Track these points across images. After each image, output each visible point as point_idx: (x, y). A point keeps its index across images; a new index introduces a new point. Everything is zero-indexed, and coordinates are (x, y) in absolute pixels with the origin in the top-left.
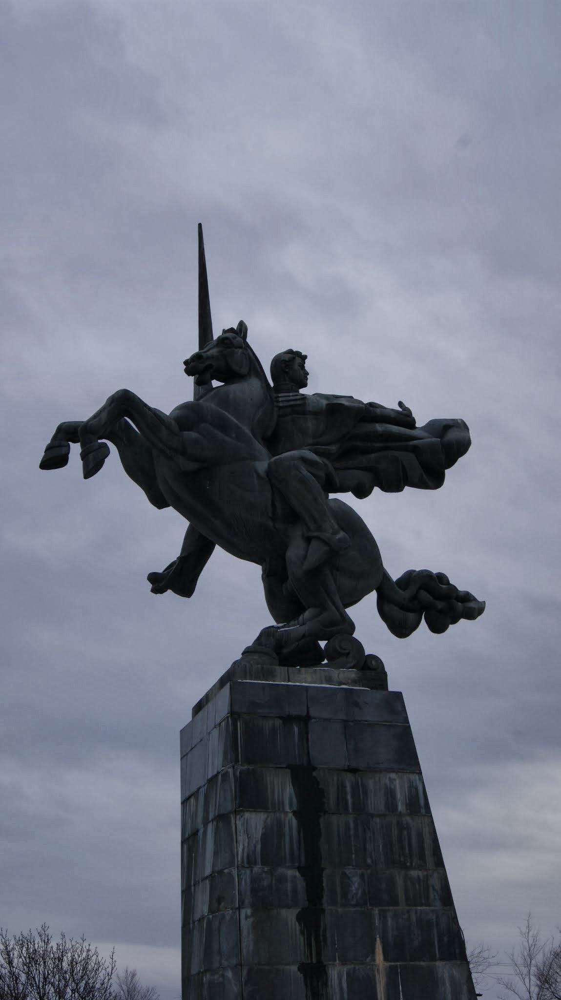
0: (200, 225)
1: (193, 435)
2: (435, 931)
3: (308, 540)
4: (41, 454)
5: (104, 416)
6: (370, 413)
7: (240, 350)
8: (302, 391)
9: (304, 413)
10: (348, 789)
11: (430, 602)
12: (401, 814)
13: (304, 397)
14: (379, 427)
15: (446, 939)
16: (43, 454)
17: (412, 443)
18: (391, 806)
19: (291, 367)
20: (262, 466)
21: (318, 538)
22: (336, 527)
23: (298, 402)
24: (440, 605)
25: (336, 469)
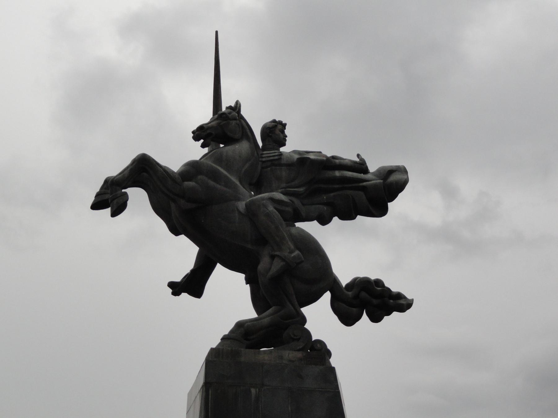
0: (217, 32)
1: (191, 184)
3: (273, 257)
4: (91, 199)
5: (126, 172)
6: (331, 164)
7: (234, 122)
8: (282, 149)
9: (281, 165)
11: (370, 301)
13: (281, 154)
14: (337, 173)
16: (93, 199)
17: (361, 184)
19: (275, 132)
20: (241, 205)
21: (278, 256)
22: (292, 247)
23: (276, 158)
24: (375, 302)
25: (303, 205)
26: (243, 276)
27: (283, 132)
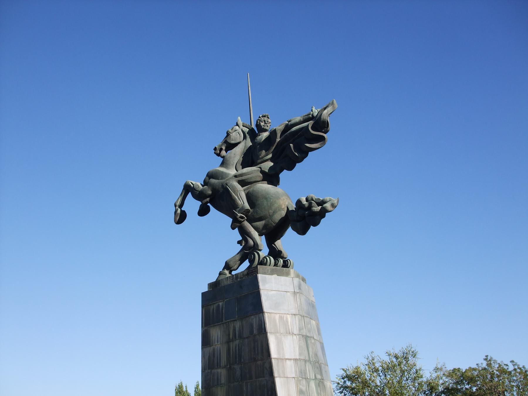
2: (266, 390)
10: (237, 329)
12: (255, 335)
15: (270, 392)
18: (251, 332)
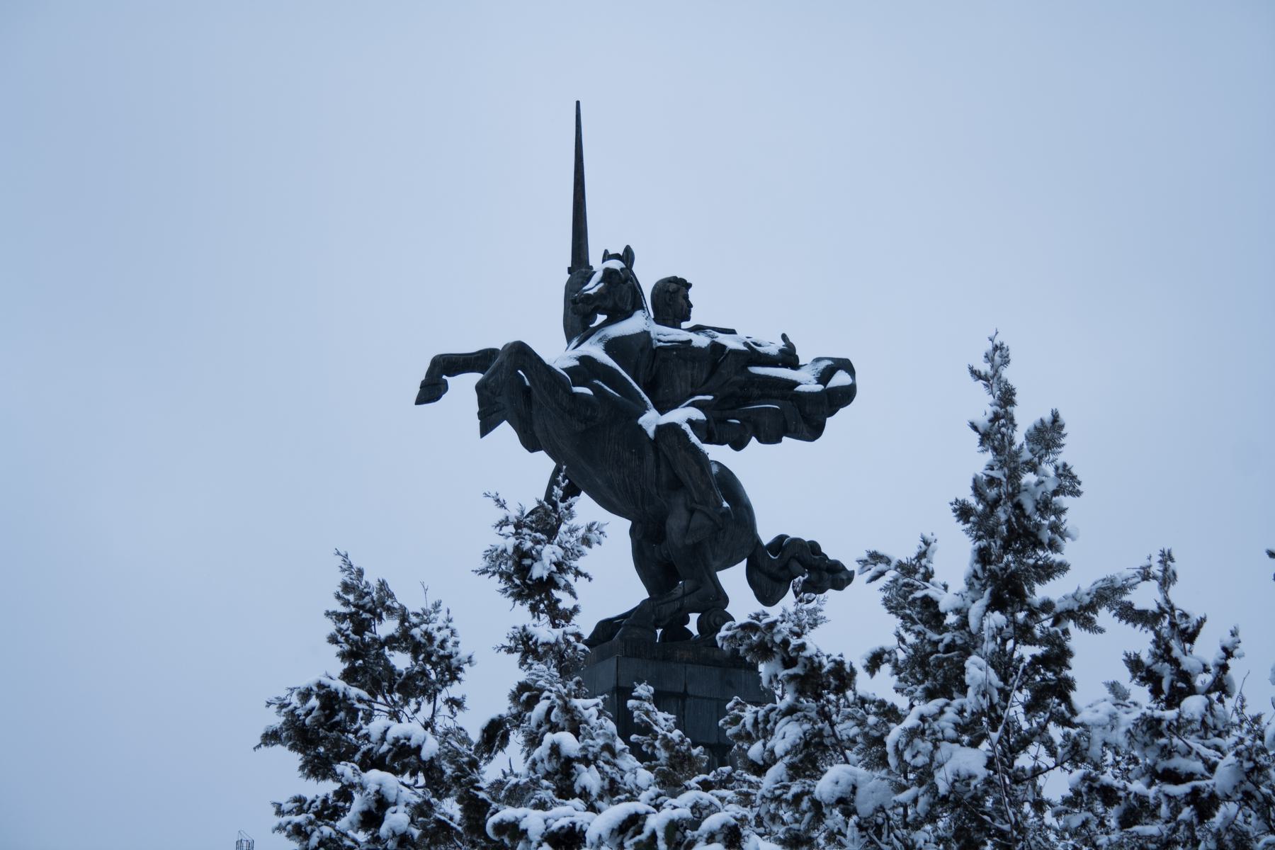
0: (578, 103)
3: (692, 512)
4: (415, 390)
26: (628, 523)
27: (686, 297)
